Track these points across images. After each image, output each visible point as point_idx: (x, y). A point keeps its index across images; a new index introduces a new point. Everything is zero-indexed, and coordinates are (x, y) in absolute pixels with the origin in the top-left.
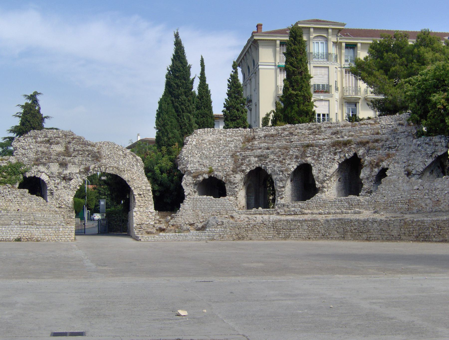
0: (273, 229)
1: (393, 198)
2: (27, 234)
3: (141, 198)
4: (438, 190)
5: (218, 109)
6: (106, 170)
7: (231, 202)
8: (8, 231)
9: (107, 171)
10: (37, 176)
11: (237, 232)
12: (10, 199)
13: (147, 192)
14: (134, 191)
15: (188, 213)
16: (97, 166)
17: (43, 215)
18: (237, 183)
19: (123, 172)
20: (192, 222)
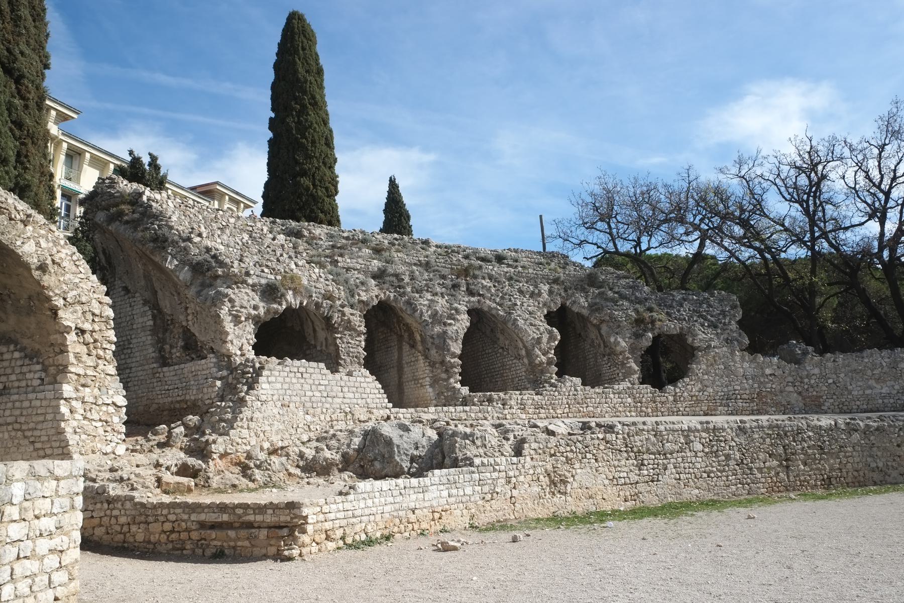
0: (625, 455)
1: (726, 390)
4: (814, 377)
14: (61, 313)
15: (269, 413)
20: (280, 444)
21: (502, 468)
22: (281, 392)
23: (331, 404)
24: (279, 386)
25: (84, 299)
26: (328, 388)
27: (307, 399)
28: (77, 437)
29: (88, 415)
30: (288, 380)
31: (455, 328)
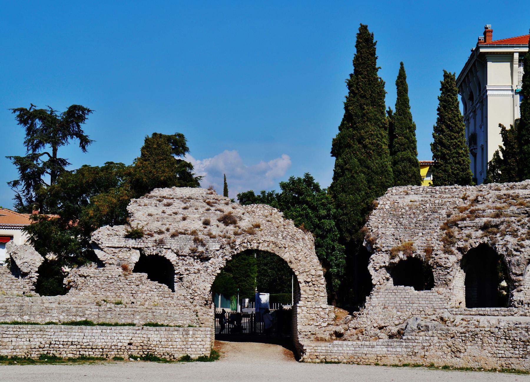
3: (309, 288)
5: (424, 153)
6: (258, 247)
7: (441, 296)
9: (260, 248)
10: (160, 254)
11: (450, 343)
12: (121, 286)
13: (318, 279)
14: (298, 277)
16: (246, 241)
17: (166, 312)
18: (449, 268)
19: (284, 249)
20: (383, 325)
21: (420, 341)
22: (383, 302)
23: (412, 307)
24: (383, 299)
25: (307, 270)
26: (410, 299)
27: (398, 305)
28: (302, 320)
29: (308, 312)
30: (387, 296)
31: (517, 258)
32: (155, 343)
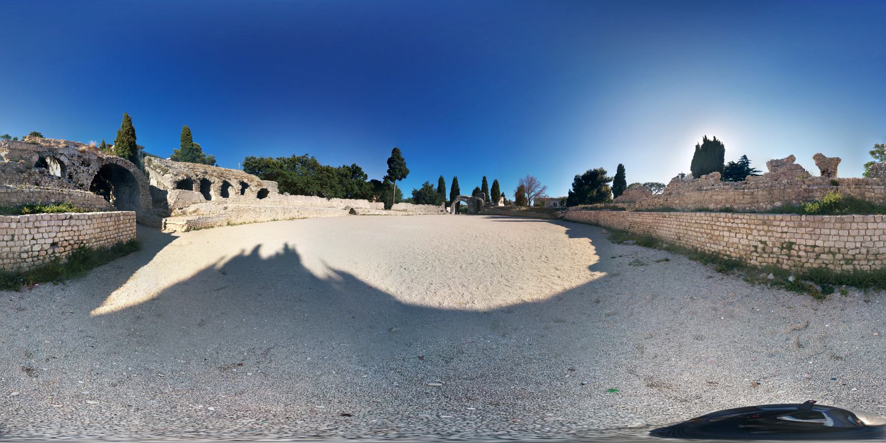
2: (72, 233)
8: (26, 231)
32: (87, 237)
